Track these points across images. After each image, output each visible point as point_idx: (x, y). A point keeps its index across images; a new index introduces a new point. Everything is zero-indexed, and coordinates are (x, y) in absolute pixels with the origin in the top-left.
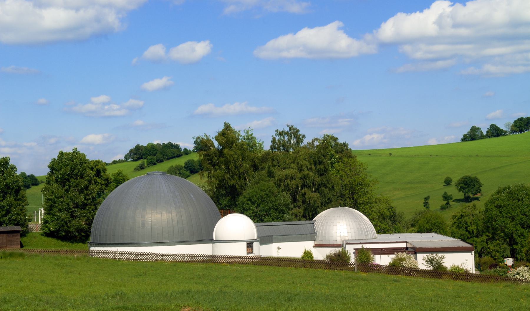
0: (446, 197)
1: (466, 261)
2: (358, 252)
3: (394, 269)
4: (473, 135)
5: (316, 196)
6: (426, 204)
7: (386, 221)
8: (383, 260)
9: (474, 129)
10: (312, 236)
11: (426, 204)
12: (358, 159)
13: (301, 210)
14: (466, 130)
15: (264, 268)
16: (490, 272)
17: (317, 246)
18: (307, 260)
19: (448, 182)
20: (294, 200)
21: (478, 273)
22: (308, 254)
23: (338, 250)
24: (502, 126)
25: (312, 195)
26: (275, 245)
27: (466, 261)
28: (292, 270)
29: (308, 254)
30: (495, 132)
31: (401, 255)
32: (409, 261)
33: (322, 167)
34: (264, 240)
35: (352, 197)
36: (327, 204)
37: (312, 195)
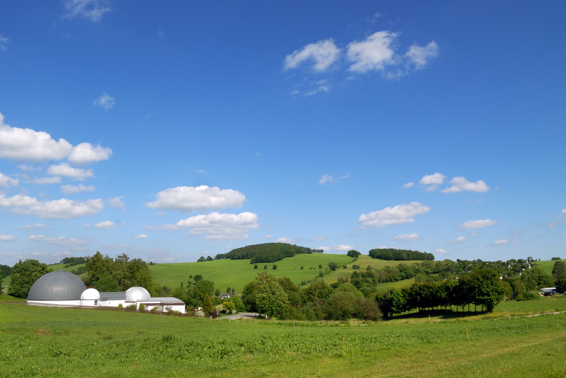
0: (189, 283)
1: (182, 309)
2: (141, 305)
3: (153, 312)
4: (201, 260)
5: (129, 282)
6: (182, 285)
7: (155, 292)
8: (150, 308)
9: (202, 257)
10: (124, 298)
11: (182, 285)
12: (150, 267)
13: (122, 288)
14: (199, 258)
15: (100, 311)
16: (190, 312)
17: (126, 302)
18: (120, 308)
19: (191, 277)
20: (120, 283)
21: (186, 313)
22: (121, 305)
23: (132, 304)
24: (212, 257)
25: (127, 282)
26: (108, 301)
27: (182, 309)
28: (112, 312)
29: (121, 305)
30: (210, 259)
31: (157, 306)
32: (160, 308)
33: (132, 271)
34: (103, 299)
35: (144, 283)
36: (133, 285)
37: (127, 282)
